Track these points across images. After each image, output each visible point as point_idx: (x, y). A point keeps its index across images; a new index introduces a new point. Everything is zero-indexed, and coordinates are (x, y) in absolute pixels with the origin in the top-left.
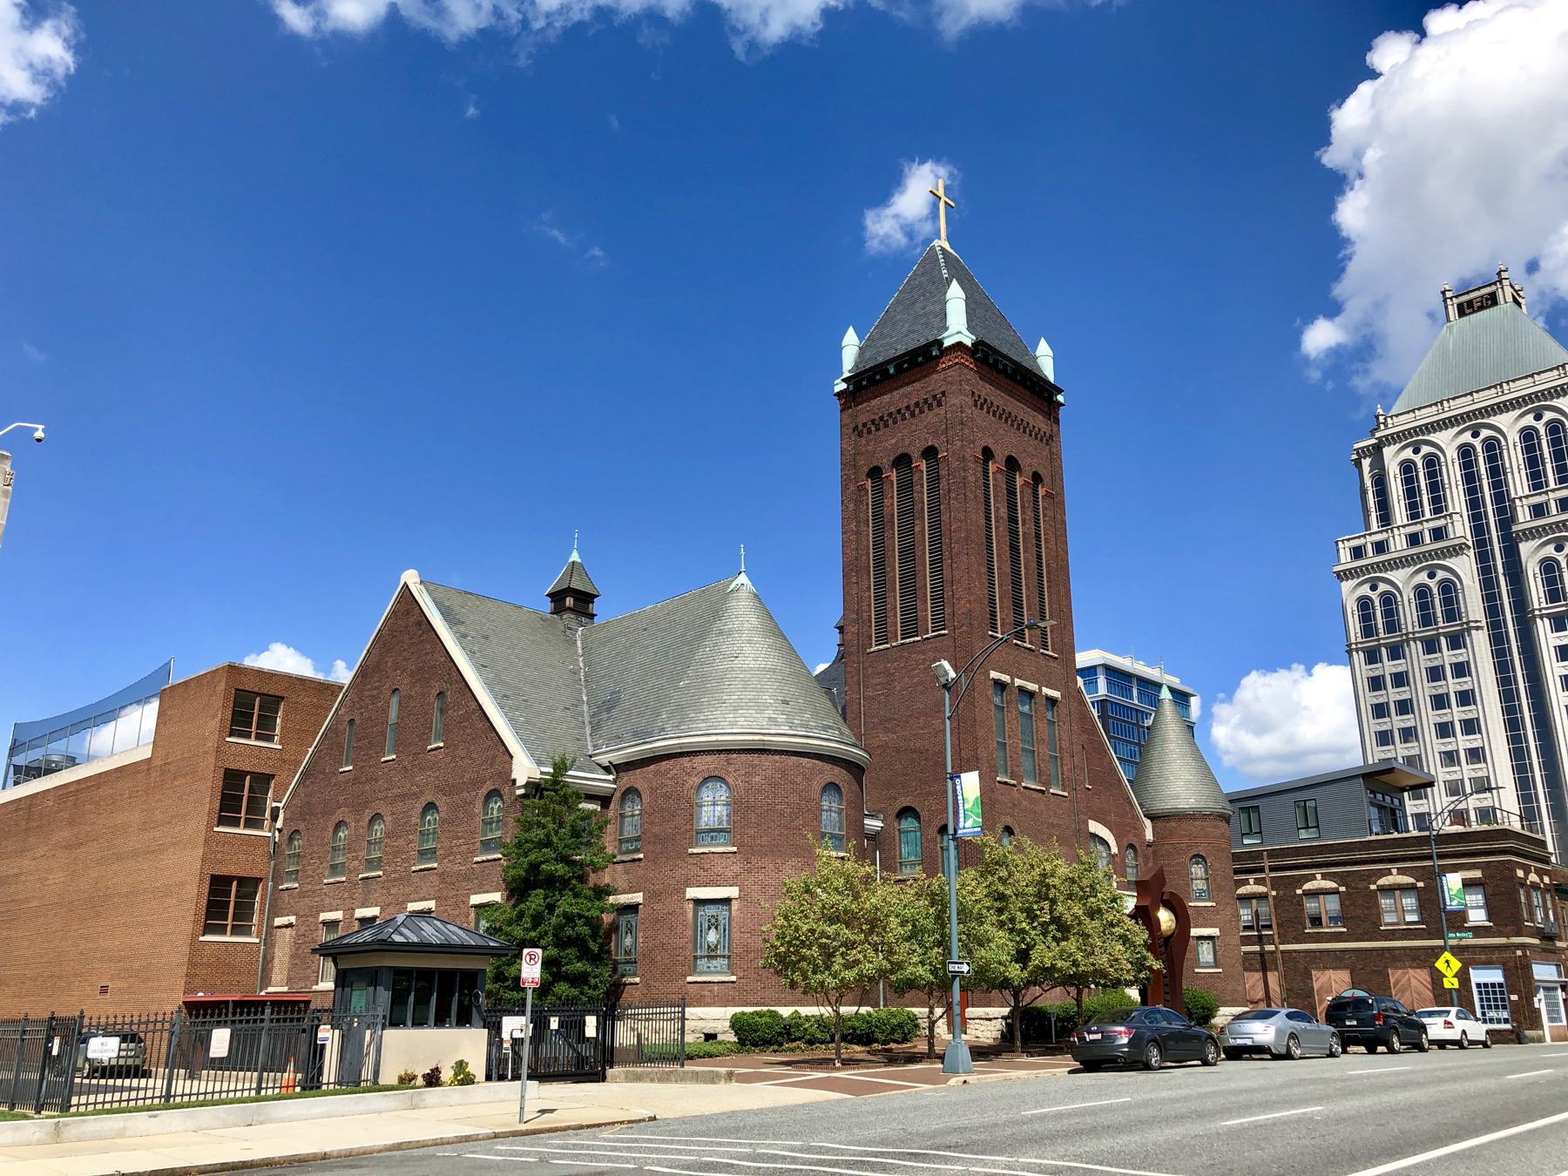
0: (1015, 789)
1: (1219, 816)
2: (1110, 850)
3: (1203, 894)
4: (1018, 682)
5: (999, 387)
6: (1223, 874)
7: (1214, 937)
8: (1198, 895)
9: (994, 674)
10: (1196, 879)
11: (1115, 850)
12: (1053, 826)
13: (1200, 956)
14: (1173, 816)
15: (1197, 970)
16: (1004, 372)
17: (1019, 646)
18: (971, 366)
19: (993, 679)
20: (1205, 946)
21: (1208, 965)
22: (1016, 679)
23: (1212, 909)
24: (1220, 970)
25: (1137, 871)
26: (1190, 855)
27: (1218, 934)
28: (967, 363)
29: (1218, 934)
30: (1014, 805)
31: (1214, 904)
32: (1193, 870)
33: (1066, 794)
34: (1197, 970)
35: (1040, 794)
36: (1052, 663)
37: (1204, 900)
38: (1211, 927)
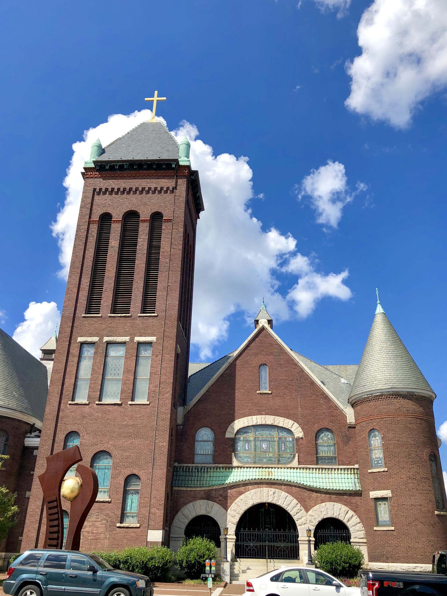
0: (87, 407)
1: (390, 395)
2: (294, 435)
3: (380, 462)
4: (106, 339)
5: (122, 178)
6: (397, 442)
7: (387, 498)
8: (376, 462)
9: (80, 339)
10: (375, 450)
11: (298, 432)
12: (127, 426)
13: (379, 516)
14: (358, 401)
15: (375, 528)
16: (121, 168)
17: (114, 317)
18: (96, 176)
19: (80, 342)
20: (383, 506)
21: (385, 523)
22: (105, 338)
23: (385, 473)
24: (393, 528)
25: (335, 448)
26: (368, 431)
27: (390, 495)
28: (96, 176)
29: (390, 495)
30: (84, 417)
31: (386, 469)
32: (372, 442)
33: (148, 403)
34: (375, 528)
35: (116, 407)
36: (151, 320)
37: (380, 467)
38: (384, 489)
